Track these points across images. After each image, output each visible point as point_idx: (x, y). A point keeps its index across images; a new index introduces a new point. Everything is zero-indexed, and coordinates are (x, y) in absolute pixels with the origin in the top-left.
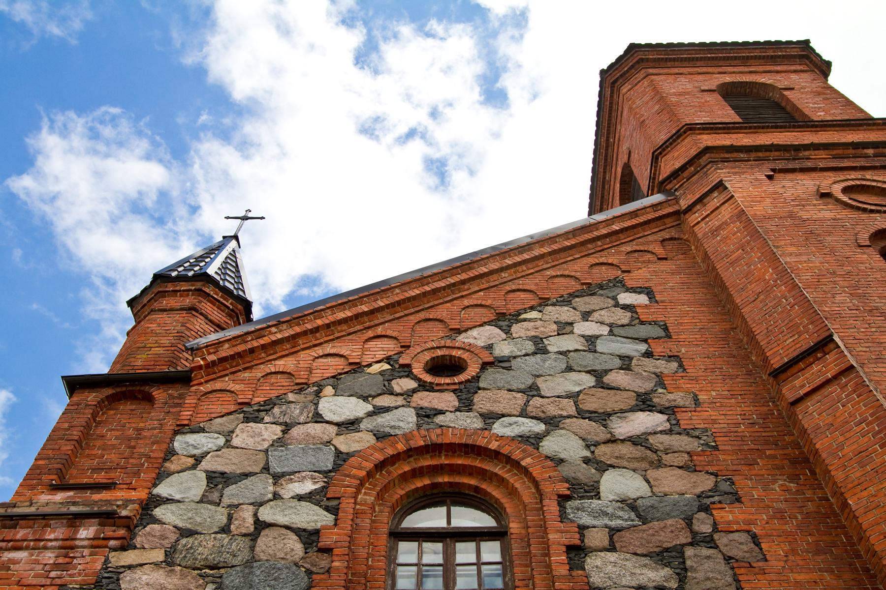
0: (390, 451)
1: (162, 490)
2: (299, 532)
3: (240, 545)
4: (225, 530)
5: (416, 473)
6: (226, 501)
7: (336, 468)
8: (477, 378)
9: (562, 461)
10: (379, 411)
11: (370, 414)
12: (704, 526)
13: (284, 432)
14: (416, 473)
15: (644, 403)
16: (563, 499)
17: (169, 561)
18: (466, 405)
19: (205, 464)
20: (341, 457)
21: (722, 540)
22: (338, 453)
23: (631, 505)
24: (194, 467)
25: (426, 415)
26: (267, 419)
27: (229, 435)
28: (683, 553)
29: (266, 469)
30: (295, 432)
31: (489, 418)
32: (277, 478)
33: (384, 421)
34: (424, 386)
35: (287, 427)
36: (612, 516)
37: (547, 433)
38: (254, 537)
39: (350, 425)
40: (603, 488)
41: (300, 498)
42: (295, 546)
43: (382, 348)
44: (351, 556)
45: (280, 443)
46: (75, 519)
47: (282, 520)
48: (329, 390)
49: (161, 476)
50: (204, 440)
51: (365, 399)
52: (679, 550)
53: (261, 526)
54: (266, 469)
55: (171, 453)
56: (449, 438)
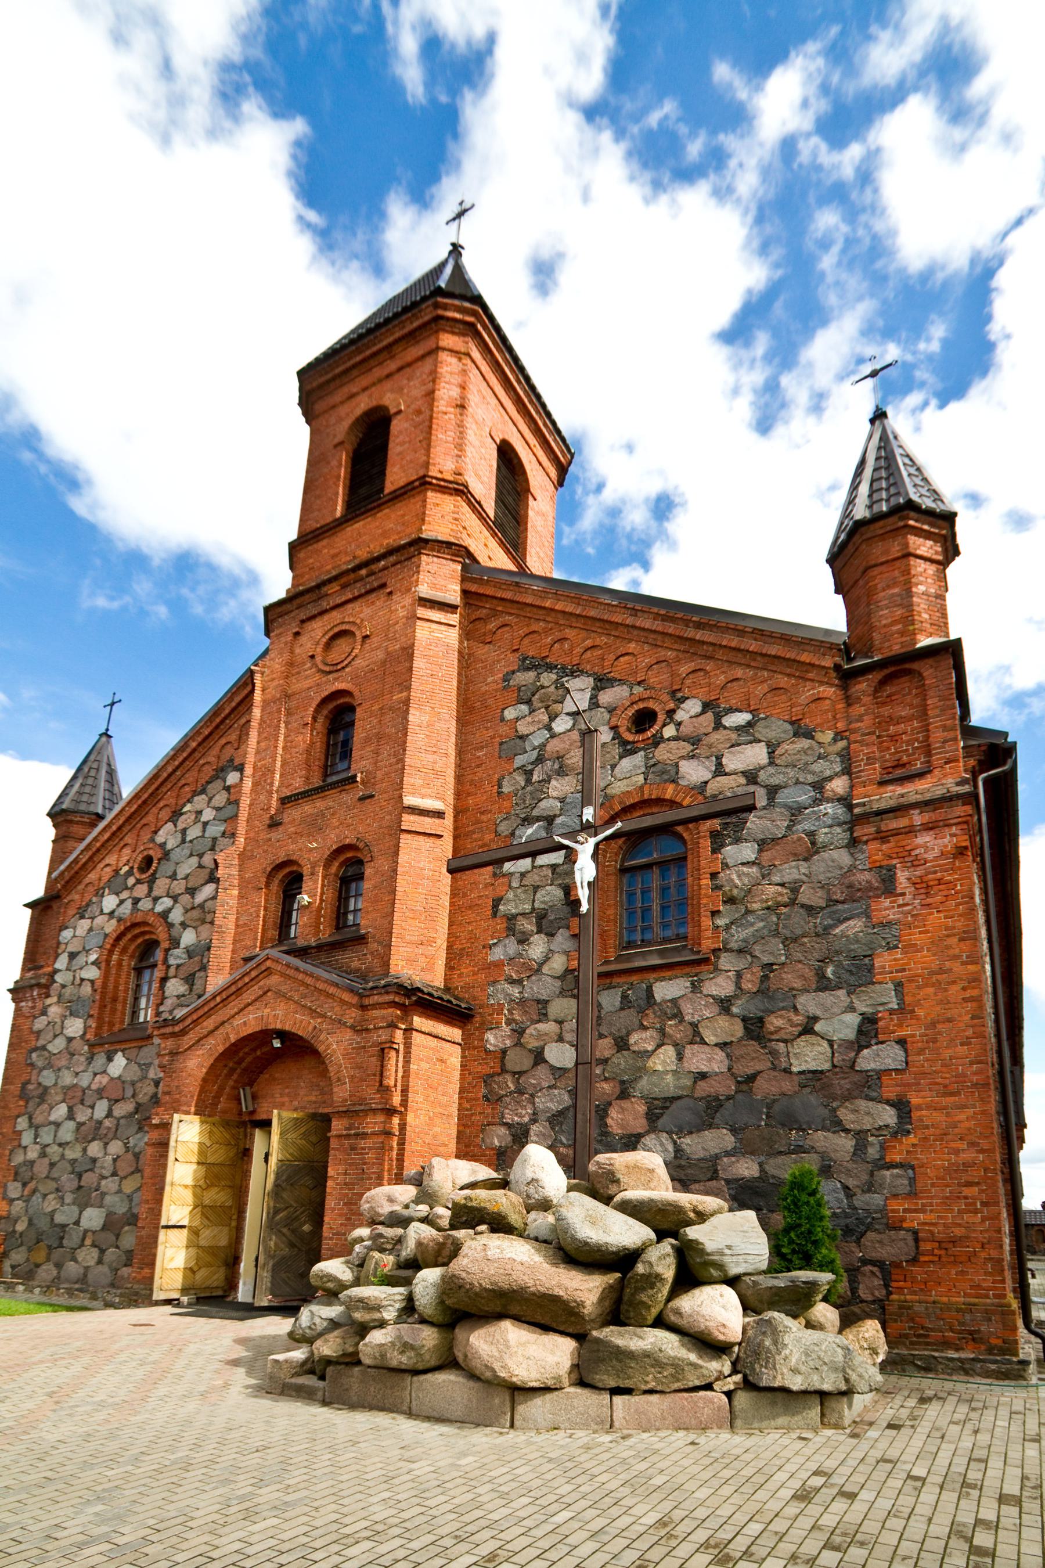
5: (136, 937)
8: (155, 872)
10: (122, 902)
14: (136, 937)
20: (106, 935)
25: (136, 901)
31: (156, 900)
53: (82, 980)
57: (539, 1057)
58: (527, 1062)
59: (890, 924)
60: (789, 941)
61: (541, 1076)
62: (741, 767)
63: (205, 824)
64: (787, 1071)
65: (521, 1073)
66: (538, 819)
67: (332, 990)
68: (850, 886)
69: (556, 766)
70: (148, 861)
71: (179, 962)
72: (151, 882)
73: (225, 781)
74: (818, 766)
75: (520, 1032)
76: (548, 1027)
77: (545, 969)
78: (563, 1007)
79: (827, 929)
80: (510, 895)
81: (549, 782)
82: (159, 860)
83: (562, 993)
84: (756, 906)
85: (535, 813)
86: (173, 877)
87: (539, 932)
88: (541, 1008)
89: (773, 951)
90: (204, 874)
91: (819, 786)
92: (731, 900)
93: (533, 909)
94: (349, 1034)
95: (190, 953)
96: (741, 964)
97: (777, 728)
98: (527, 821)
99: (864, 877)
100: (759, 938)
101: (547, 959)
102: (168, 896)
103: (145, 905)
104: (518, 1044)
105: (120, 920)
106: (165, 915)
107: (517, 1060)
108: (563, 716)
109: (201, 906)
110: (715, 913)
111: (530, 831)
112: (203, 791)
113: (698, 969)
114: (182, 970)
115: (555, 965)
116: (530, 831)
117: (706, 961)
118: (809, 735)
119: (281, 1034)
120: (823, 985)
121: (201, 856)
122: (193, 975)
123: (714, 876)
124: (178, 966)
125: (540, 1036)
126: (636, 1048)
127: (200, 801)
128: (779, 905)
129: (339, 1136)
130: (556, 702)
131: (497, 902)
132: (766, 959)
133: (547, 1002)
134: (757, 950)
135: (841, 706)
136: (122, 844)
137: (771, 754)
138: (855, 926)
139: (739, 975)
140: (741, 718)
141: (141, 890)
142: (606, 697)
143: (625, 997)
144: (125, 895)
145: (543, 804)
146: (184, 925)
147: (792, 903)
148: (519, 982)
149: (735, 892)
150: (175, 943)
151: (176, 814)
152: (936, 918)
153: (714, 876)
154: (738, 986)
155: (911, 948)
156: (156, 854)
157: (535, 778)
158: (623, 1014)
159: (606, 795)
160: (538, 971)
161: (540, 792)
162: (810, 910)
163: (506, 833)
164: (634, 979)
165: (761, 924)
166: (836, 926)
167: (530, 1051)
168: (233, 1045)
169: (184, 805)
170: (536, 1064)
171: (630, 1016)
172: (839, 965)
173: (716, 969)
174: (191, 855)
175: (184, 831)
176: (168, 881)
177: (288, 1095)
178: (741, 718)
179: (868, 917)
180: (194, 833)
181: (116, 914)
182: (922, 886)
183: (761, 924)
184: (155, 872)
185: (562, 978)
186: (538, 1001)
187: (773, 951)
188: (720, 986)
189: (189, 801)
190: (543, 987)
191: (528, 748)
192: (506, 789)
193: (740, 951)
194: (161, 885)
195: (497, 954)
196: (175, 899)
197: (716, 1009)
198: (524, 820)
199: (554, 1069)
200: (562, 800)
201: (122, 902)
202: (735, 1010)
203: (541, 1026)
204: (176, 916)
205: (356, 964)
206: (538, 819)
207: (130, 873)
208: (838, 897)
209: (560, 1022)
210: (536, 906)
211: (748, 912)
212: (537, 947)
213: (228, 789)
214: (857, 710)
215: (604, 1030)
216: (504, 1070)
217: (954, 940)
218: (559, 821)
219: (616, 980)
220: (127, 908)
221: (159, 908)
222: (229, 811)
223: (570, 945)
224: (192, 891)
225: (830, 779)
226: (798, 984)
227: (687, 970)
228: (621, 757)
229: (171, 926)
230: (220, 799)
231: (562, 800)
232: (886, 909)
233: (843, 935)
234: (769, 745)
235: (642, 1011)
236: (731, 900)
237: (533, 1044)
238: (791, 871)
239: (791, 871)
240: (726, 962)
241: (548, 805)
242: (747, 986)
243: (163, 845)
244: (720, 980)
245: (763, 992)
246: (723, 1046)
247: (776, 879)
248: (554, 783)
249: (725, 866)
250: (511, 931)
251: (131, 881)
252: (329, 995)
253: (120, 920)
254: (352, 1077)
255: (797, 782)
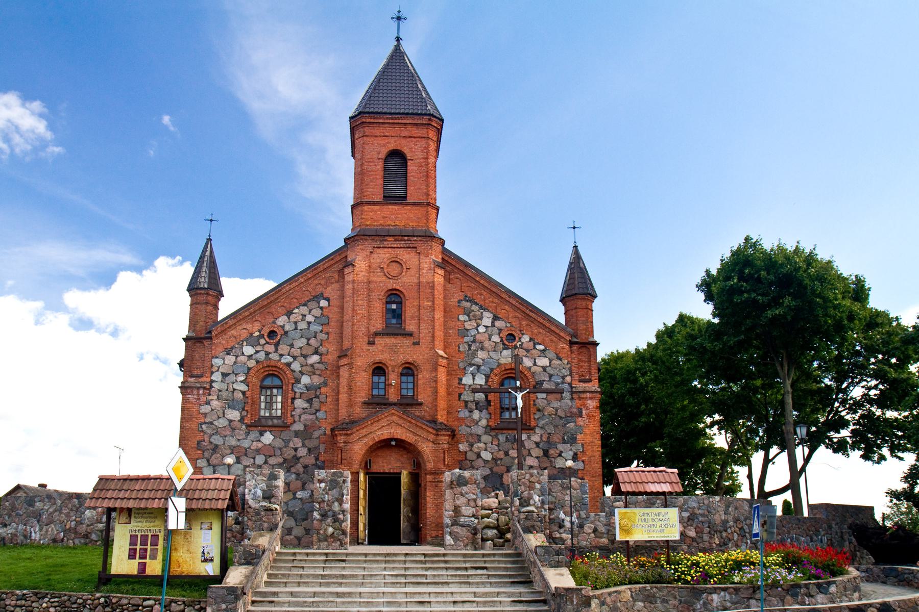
0: (259, 368)
1: (213, 378)
2: (241, 391)
3: (231, 394)
4: (227, 390)
6: (226, 382)
7: (248, 372)
9: (295, 371)
10: (257, 352)
11: (255, 353)
12: (318, 394)
13: (236, 358)
15: (316, 352)
16: (293, 384)
17: (218, 399)
18: (276, 350)
19: (220, 370)
20: (249, 369)
21: (320, 397)
22: (248, 367)
23: (306, 386)
24: (218, 371)
25: (267, 354)
26: (232, 354)
27: (224, 359)
28: (312, 401)
29: (233, 372)
30: (239, 358)
31: (281, 355)
32: (236, 375)
33: (258, 355)
34: (267, 343)
35: (237, 357)
36: (302, 389)
37: (293, 361)
38: (233, 392)
39: (250, 357)
40: (302, 381)
41: (241, 382)
42: (241, 395)
43: (257, 326)
44: (252, 399)
45: (235, 363)
46: (198, 388)
47: (238, 388)
48: (245, 343)
49: (212, 373)
50: (219, 362)
51: (253, 346)
52: (312, 399)
53: (234, 390)
54: (233, 372)
55: (212, 365)
56: (272, 363)
57: (479, 456)
58: (474, 457)
59: (580, 426)
60: (556, 426)
61: (480, 462)
62: (542, 365)
63: (309, 323)
64: (555, 467)
65: (472, 461)
66: (474, 365)
67: (424, 427)
68: (571, 412)
69: (480, 346)
70: (272, 334)
71: (302, 391)
72: (277, 345)
73: (319, 303)
74: (563, 371)
75: (471, 445)
76: (481, 445)
77: (479, 424)
78: (485, 438)
79: (565, 425)
80: (465, 393)
81: (477, 351)
82: (281, 335)
83: (486, 433)
84: (546, 414)
85: (473, 362)
86: (292, 346)
87: (476, 409)
88: (479, 438)
89: (550, 429)
90: (311, 350)
91: (563, 377)
92: (539, 410)
93: (474, 400)
94: (431, 444)
95: (308, 388)
96: (542, 432)
97: (551, 354)
98: (471, 365)
99: (575, 410)
100: (547, 424)
101: (480, 420)
102: (289, 355)
103: (274, 357)
104: (471, 450)
105: (257, 362)
106: (288, 365)
107: (471, 456)
108: (482, 326)
109: (312, 365)
110: (534, 414)
111: (471, 369)
112: (305, 305)
113: (530, 431)
114: (303, 396)
115: (483, 423)
116: (471, 369)
117: (532, 429)
118: (560, 360)
119: (396, 440)
120: (564, 442)
121: (308, 339)
122: (312, 399)
123: (534, 401)
124: (301, 393)
125: (478, 448)
126: (511, 456)
127: (304, 310)
128: (552, 414)
129: (430, 482)
130: (479, 319)
131: (460, 395)
132: (549, 431)
133: (480, 436)
134: (546, 428)
135: (569, 353)
136: (254, 319)
137: (550, 362)
138: (572, 425)
139: (541, 435)
140: (541, 347)
141: (270, 348)
142: (498, 324)
143: (507, 438)
144: (258, 348)
145: (476, 359)
146: (302, 373)
147: (556, 414)
148: (470, 427)
149: (540, 408)
150: (298, 381)
151: (289, 313)
152: (592, 426)
153: (534, 401)
154: (541, 438)
155: (585, 434)
156: (280, 332)
157: (472, 348)
158: (507, 443)
159: (498, 363)
160: (477, 424)
161: (474, 355)
162: (561, 418)
163: (462, 367)
164: (510, 432)
165: (547, 420)
166: (567, 424)
167: (475, 453)
168: (376, 442)
169: (294, 309)
170: (478, 458)
171: (508, 445)
172: (568, 436)
173: (535, 432)
174: (302, 337)
175: (296, 323)
176: (289, 347)
177: (386, 463)
178: (541, 347)
179: (576, 423)
180: (302, 325)
181: (253, 357)
182: (588, 415)
183: (547, 420)
184: (279, 340)
185: (486, 428)
186: (478, 435)
187: (550, 429)
188: (536, 438)
189: (297, 307)
190: (480, 431)
191: (469, 335)
192: (461, 349)
193: (541, 428)
194: (284, 349)
195: (461, 415)
196: (295, 358)
197: (534, 446)
198: (469, 364)
199: (484, 460)
200: (483, 360)
201: (257, 352)
202: (540, 446)
203: (479, 444)
204: (296, 366)
205: (417, 414)
206: (474, 365)
207: (261, 336)
208: (568, 415)
209: (485, 444)
210: (476, 399)
211: (544, 415)
212: (476, 415)
213: (322, 308)
214: (574, 356)
215: (501, 448)
216: (466, 459)
217: (595, 434)
218: (483, 368)
219: (504, 431)
220: (261, 356)
221: (284, 360)
222: (324, 320)
223: (488, 416)
224: (305, 357)
225: (566, 376)
226: (557, 441)
227: (526, 431)
228: (503, 349)
229: (294, 371)
230: (317, 312)
231: (483, 360)
232: (580, 421)
233: (569, 427)
234: (549, 359)
235: (513, 443)
236: (539, 410)
237: (476, 450)
238: (556, 404)
239: (556, 404)
240: (537, 430)
241: (477, 360)
242: (544, 439)
243: (283, 327)
244: (536, 436)
245: (548, 442)
246: (537, 457)
247: (552, 406)
248: (479, 352)
249: (537, 398)
250: (466, 406)
251: (262, 341)
252: (422, 428)
253: (257, 362)
254: (434, 460)
255: (557, 375)
